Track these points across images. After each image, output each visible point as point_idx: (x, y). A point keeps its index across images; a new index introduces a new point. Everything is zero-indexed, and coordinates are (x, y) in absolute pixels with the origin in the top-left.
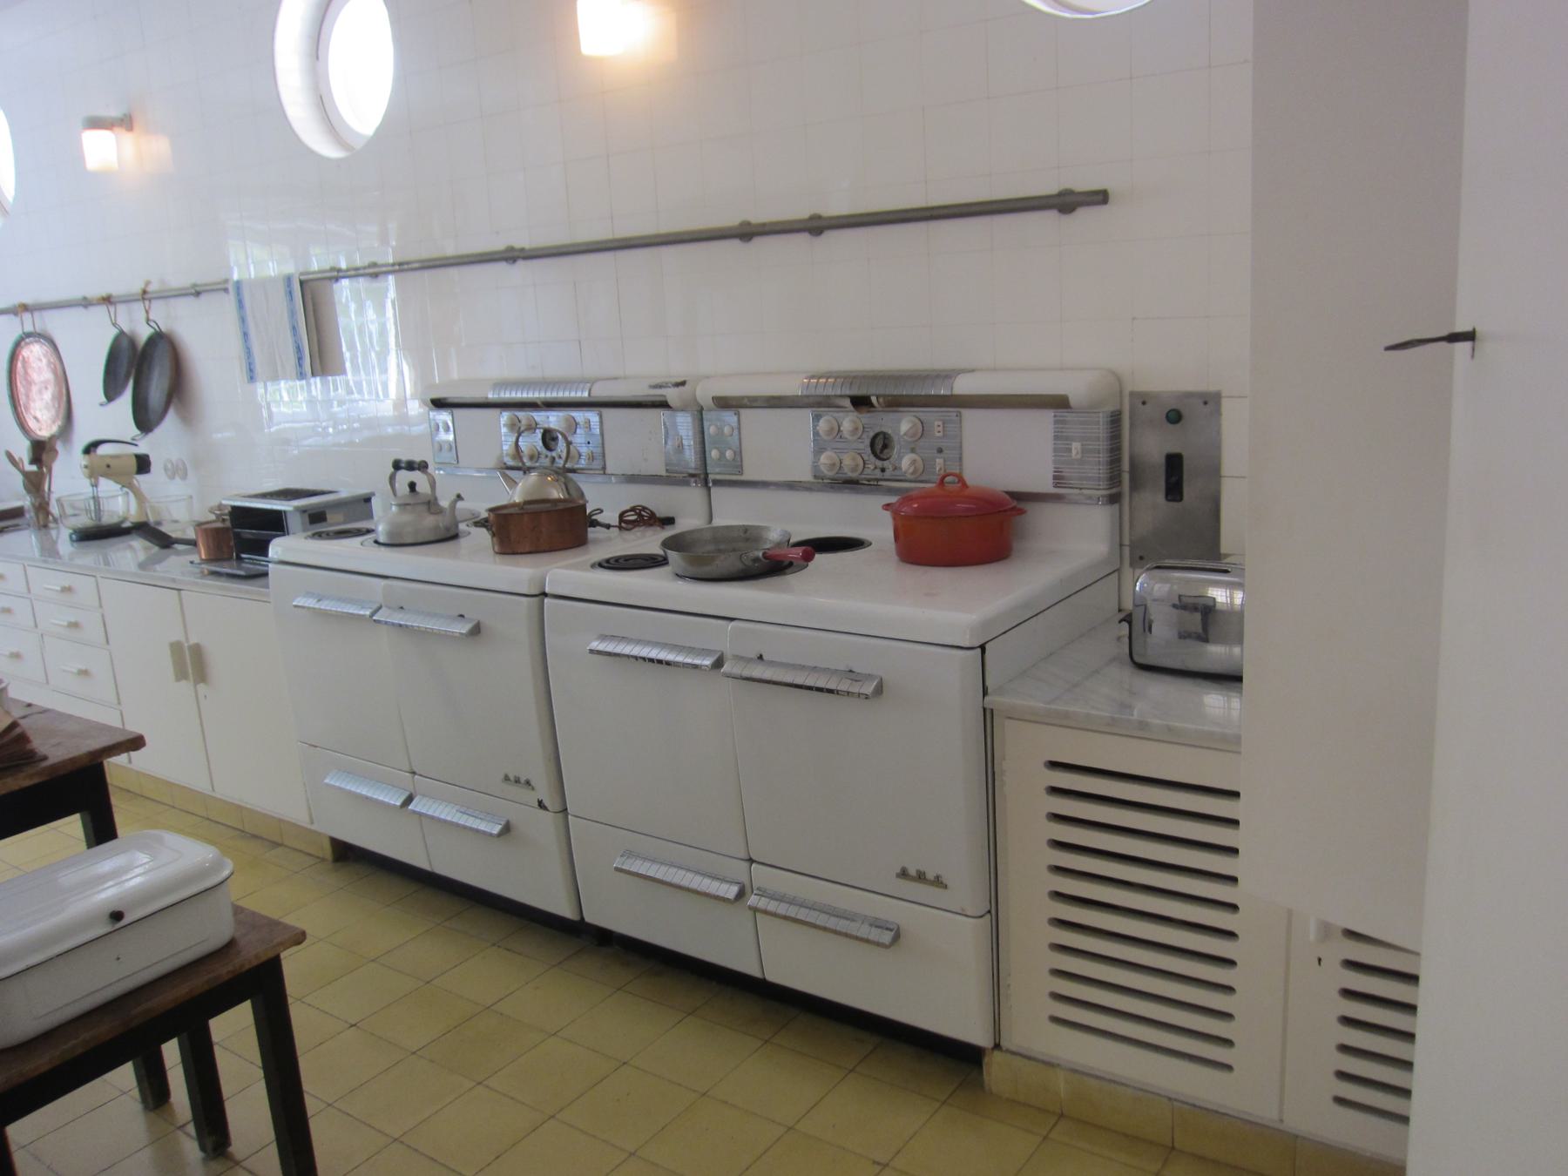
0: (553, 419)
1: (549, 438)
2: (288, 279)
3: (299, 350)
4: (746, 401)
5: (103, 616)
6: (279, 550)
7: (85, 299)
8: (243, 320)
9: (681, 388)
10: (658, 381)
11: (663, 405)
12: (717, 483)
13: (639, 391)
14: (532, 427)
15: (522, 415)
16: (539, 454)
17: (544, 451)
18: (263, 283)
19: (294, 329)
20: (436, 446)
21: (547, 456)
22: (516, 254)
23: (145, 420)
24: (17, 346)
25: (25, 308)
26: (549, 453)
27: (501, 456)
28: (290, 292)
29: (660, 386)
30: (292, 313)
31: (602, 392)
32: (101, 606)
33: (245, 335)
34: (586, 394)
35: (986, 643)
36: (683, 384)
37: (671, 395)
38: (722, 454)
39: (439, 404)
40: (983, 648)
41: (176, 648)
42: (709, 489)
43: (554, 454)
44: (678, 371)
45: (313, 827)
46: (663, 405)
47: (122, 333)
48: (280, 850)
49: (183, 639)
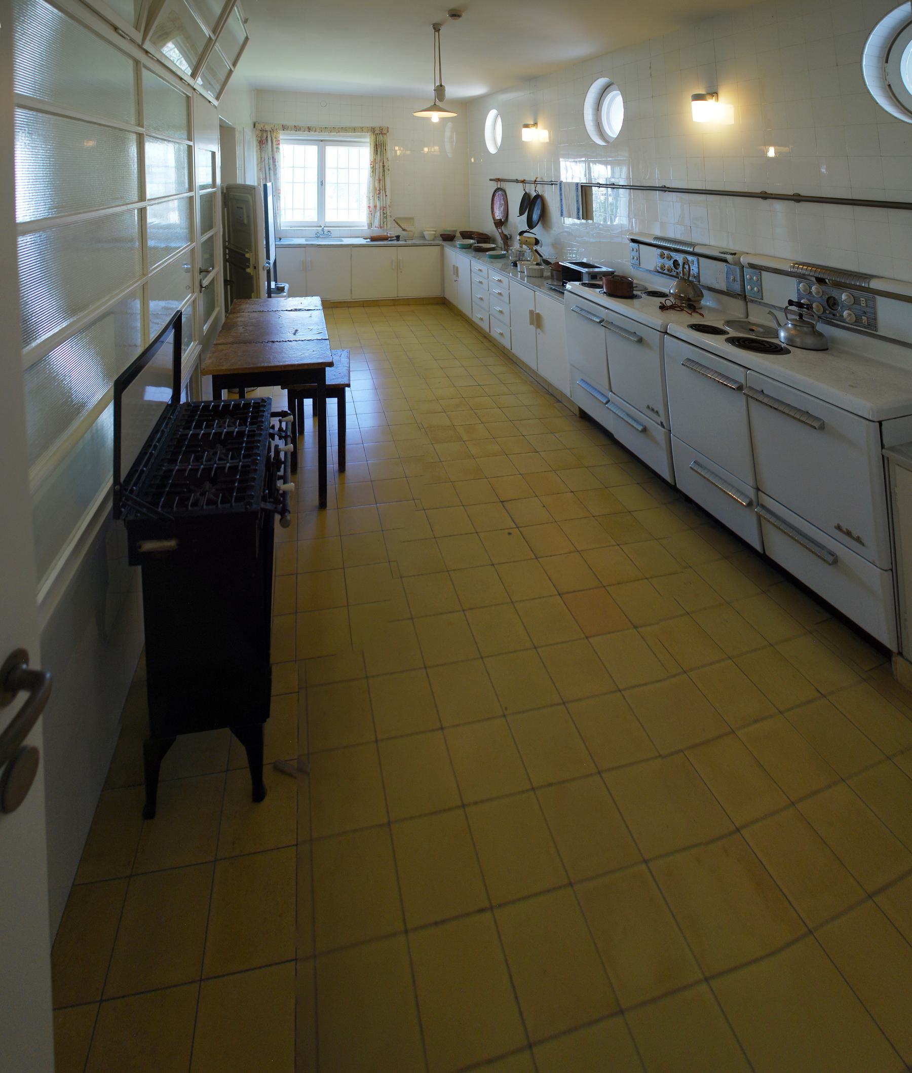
0: (680, 258)
1: (676, 263)
2: (577, 184)
3: (578, 209)
4: (763, 268)
5: (509, 293)
6: (570, 287)
7: (517, 180)
8: (561, 194)
9: (733, 256)
10: (725, 250)
11: (725, 261)
12: (752, 301)
13: (715, 253)
14: (670, 258)
15: (666, 252)
16: (672, 269)
17: (674, 269)
18: (569, 184)
19: (577, 201)
20: (632, 257)
21: (675, 271)
22: (666, 189)
23: (531, 224)
24: (495, 191)
25: (498, 180)
26: (676, 270)
27: (656, 267)
28: (577, 189)
29: (724, 253)
30: (577, 196)
31: (698, 250)
32: (509, 289)
33: (561, 200)
34: (691, 250)
35: (883, 421)
36: (735, 254)
37: (729, 257)
38: (752, 289)
39: (633, 241)
40: (880, 423)
41: (531, 312)
42: (747, 302)
43: (678, 271)
44: (732, 247)
45: (571, 399)
46: (725, 261)
47: (526, 193)
48: (561, 404)
49: (534, 309)
